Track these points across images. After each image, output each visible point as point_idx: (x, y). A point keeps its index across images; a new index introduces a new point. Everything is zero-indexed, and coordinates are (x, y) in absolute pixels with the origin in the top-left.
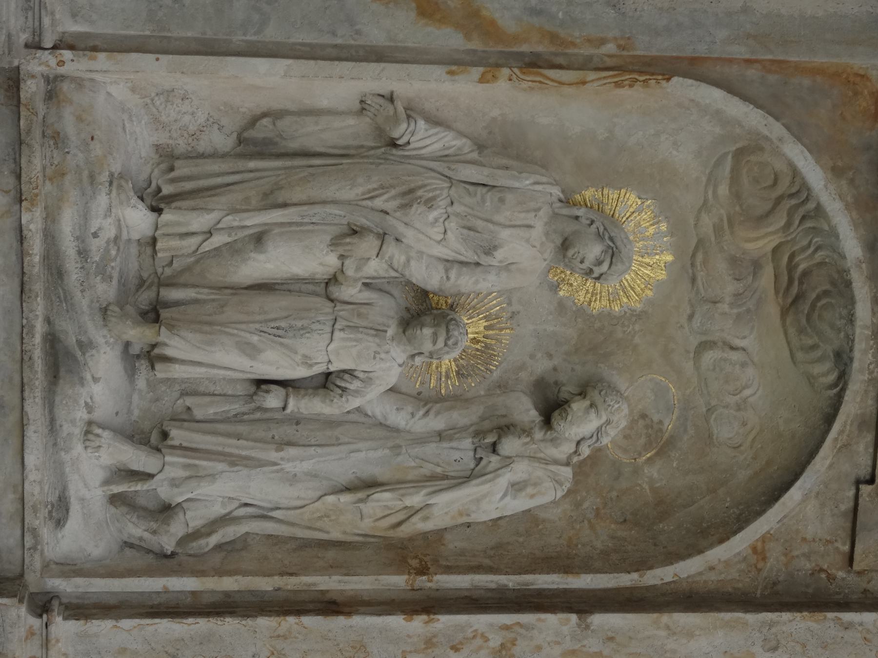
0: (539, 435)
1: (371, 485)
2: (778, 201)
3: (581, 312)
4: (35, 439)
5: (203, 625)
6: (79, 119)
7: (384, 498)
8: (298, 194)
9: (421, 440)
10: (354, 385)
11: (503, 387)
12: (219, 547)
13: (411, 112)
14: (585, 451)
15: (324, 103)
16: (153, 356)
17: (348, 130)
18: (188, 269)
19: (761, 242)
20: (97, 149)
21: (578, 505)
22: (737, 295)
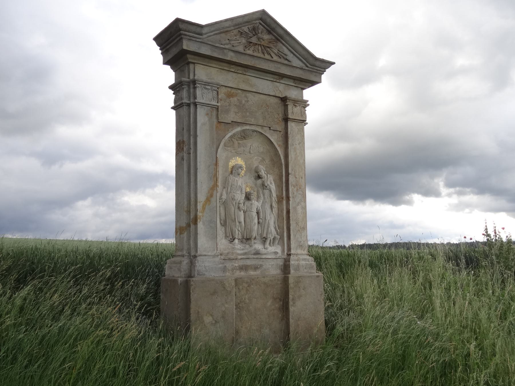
0: (263, 180)
1: (271, 206)
9: (264, 198)
11: (256, 185)
19: (236, 142)
21: (271, 174)
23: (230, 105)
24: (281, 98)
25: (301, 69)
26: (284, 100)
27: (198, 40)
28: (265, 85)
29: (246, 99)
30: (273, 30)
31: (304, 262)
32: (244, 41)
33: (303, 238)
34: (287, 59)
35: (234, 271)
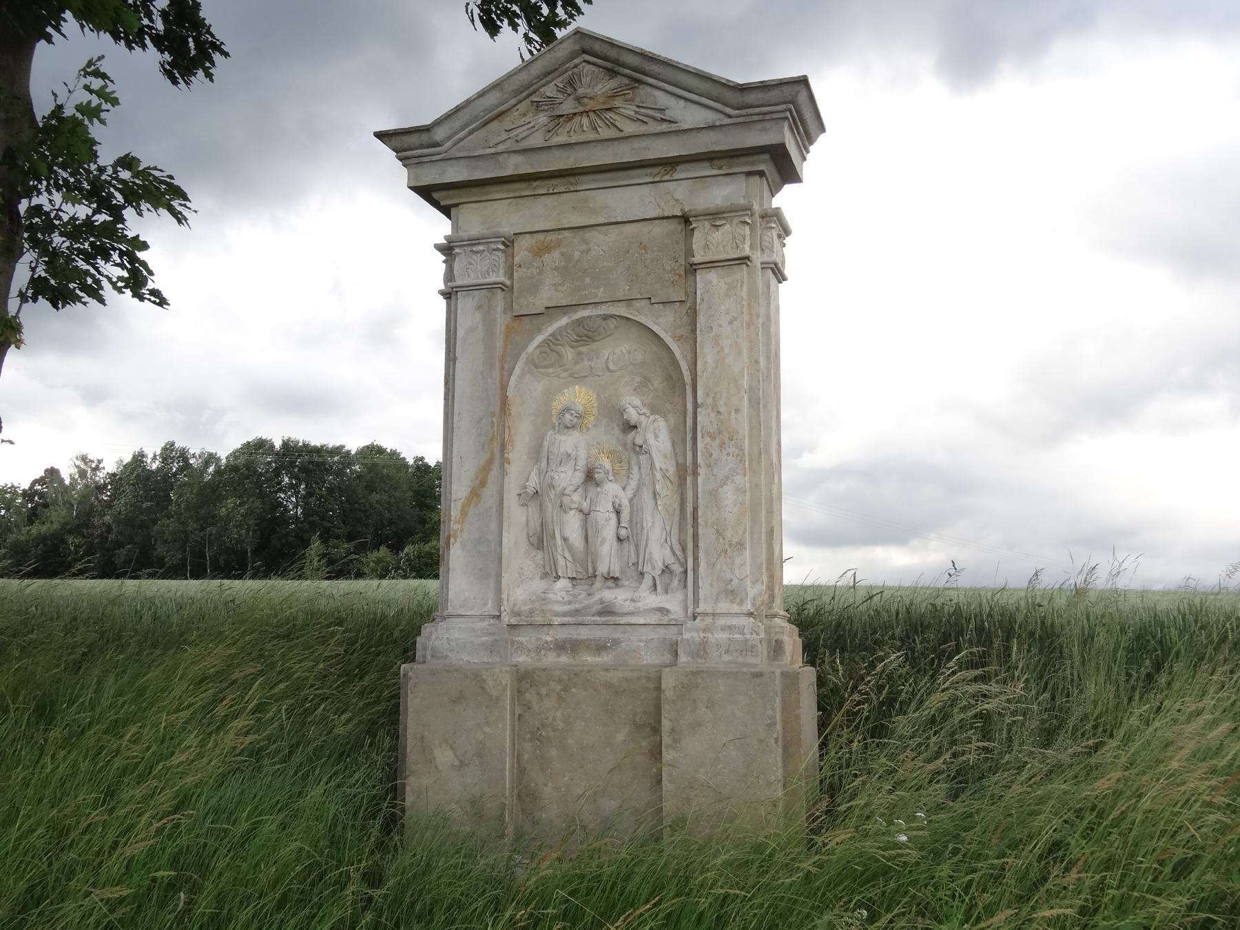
4: (634, 620)
5: (701, 554)
11: (625, 446)
19: (569, 354)
28: (634, 200)
29: (584, 247)
31: (723, 636)
33: (737, 572)
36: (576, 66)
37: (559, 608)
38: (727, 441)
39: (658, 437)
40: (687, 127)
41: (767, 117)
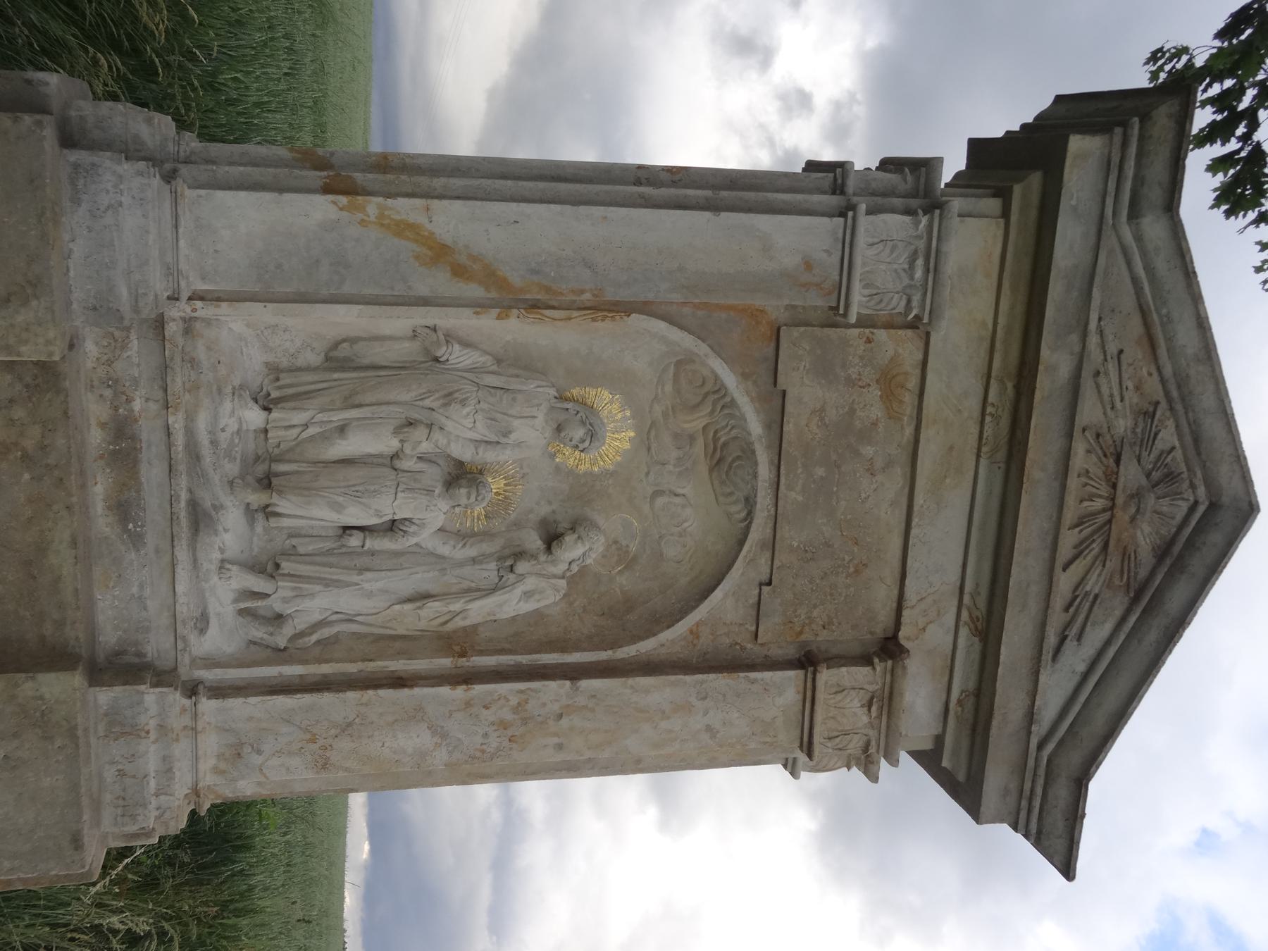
0: (543, 558)
1: (426, 597)
2: (706, 395)
3: (571, 473)
4: (183, 574)
6: (209, 349)
7: (434, 606)
8: (369, 398)
9: (461, 564)
10: (413, 529)
11: (518, 525)
12: (318, 642)
13: (450, 338)
14: (575, 568)
15: (387, 332)
16: (268, 512)
17: (405, 350)
18: (291, 450)
19: (695, 423)
20: (223, 370)
21: (571, 604)
22: (679, 459)
23: (850, 382)
24: (895, 637)
25: (1030, 716)
26: (889, 648)
27: (1110, 201)
29: (879, 463)
30: (1178, 567)
31: (152, 763)
32: (1122, 425)
33: (275, 761)
34: (1063, 639)
35: (108, 393)
36: (1193, 486)
37: (202, 422)
38: (510, 732)
39: (531, 595)
40: (1042, 678)
41: (1024, 803)
